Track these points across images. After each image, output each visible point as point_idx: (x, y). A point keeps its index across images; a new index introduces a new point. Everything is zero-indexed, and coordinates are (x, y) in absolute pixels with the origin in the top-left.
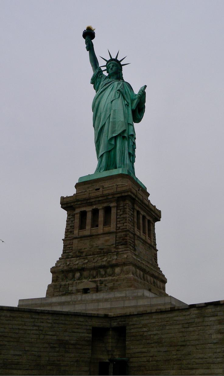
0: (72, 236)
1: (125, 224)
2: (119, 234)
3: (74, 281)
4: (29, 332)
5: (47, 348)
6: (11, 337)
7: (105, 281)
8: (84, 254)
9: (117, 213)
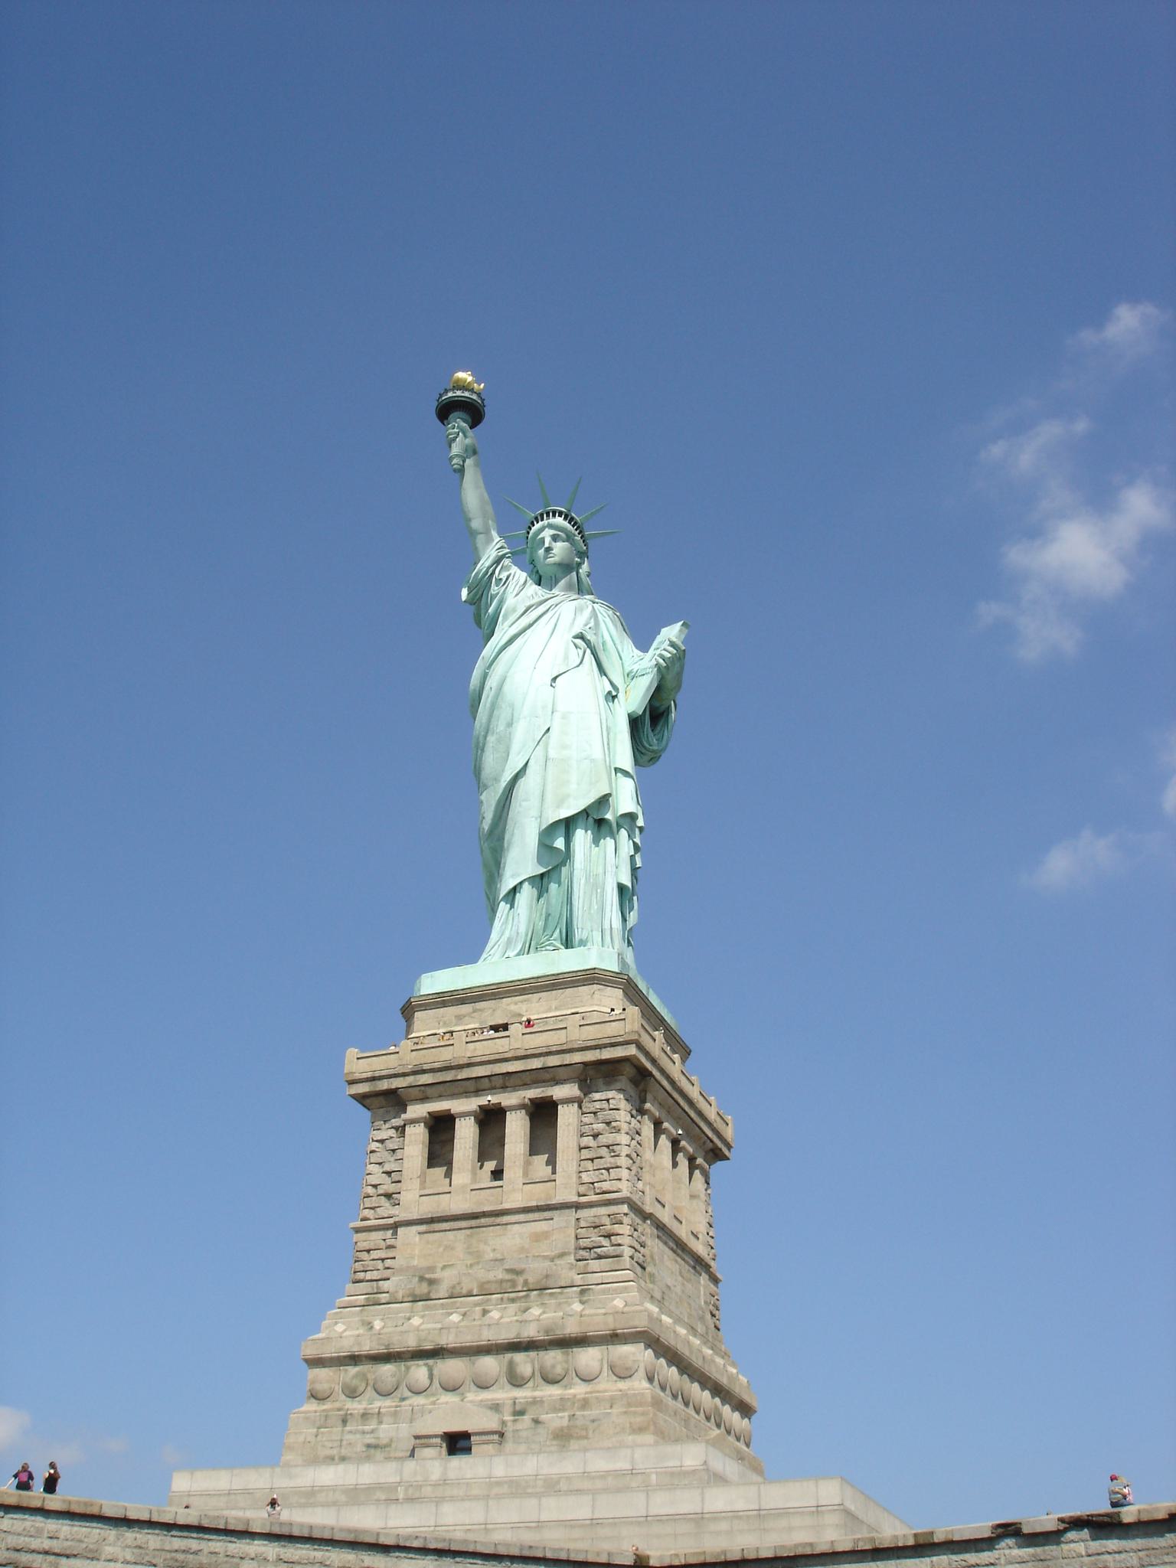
0: (395, 1211)
2: (584, 1213)
3: (403, 1399)
7: (535, 1402)
8: (442, 1290)
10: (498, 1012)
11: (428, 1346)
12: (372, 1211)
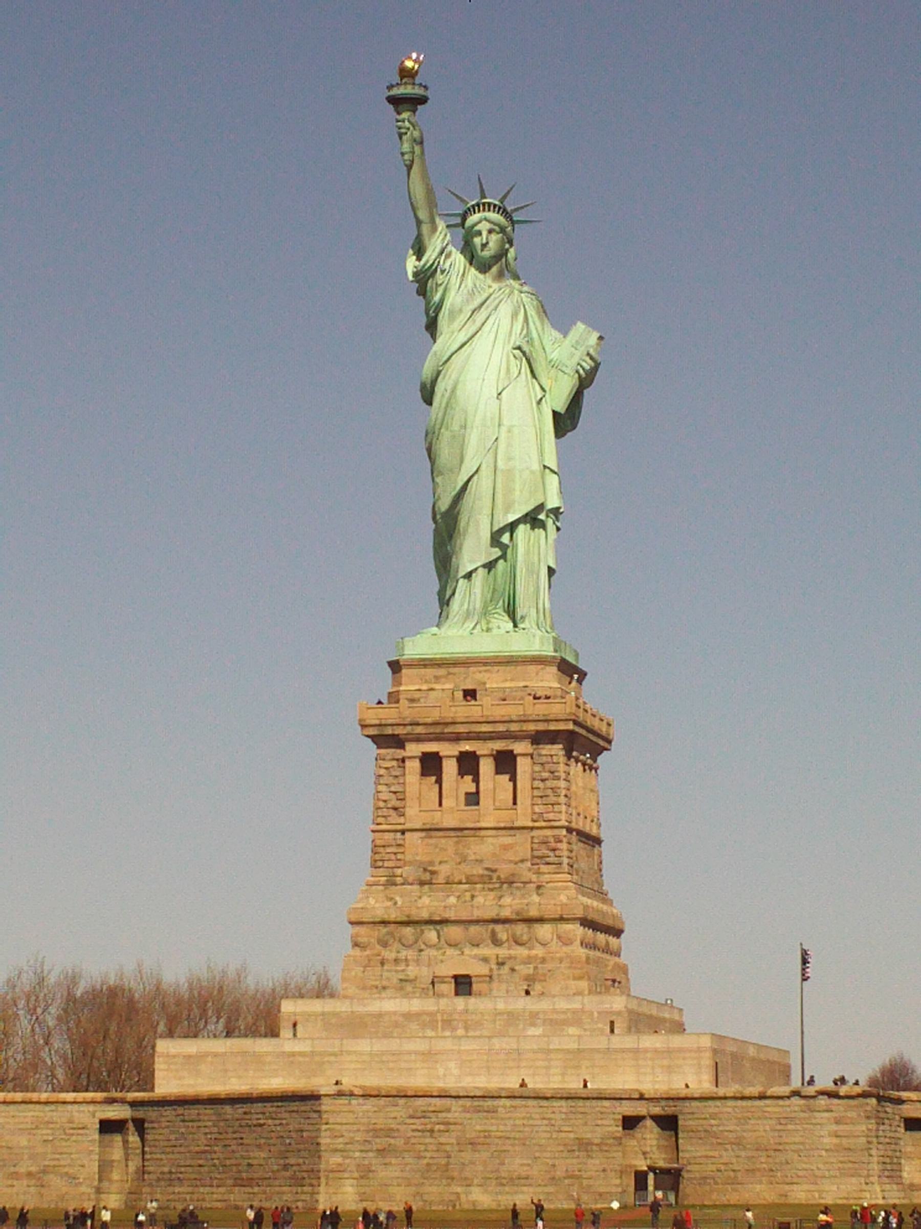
0: (402, 820)
1: (556, 808)
3: (421, 951)
4: (536, 1129)
5: (562, 1151)
6: (515, 1139)
7: (510, 958)
8: (441, 879)
9: (533, 772)
10: (469, 680)
11: (438, 918)
12: (383, 819)
